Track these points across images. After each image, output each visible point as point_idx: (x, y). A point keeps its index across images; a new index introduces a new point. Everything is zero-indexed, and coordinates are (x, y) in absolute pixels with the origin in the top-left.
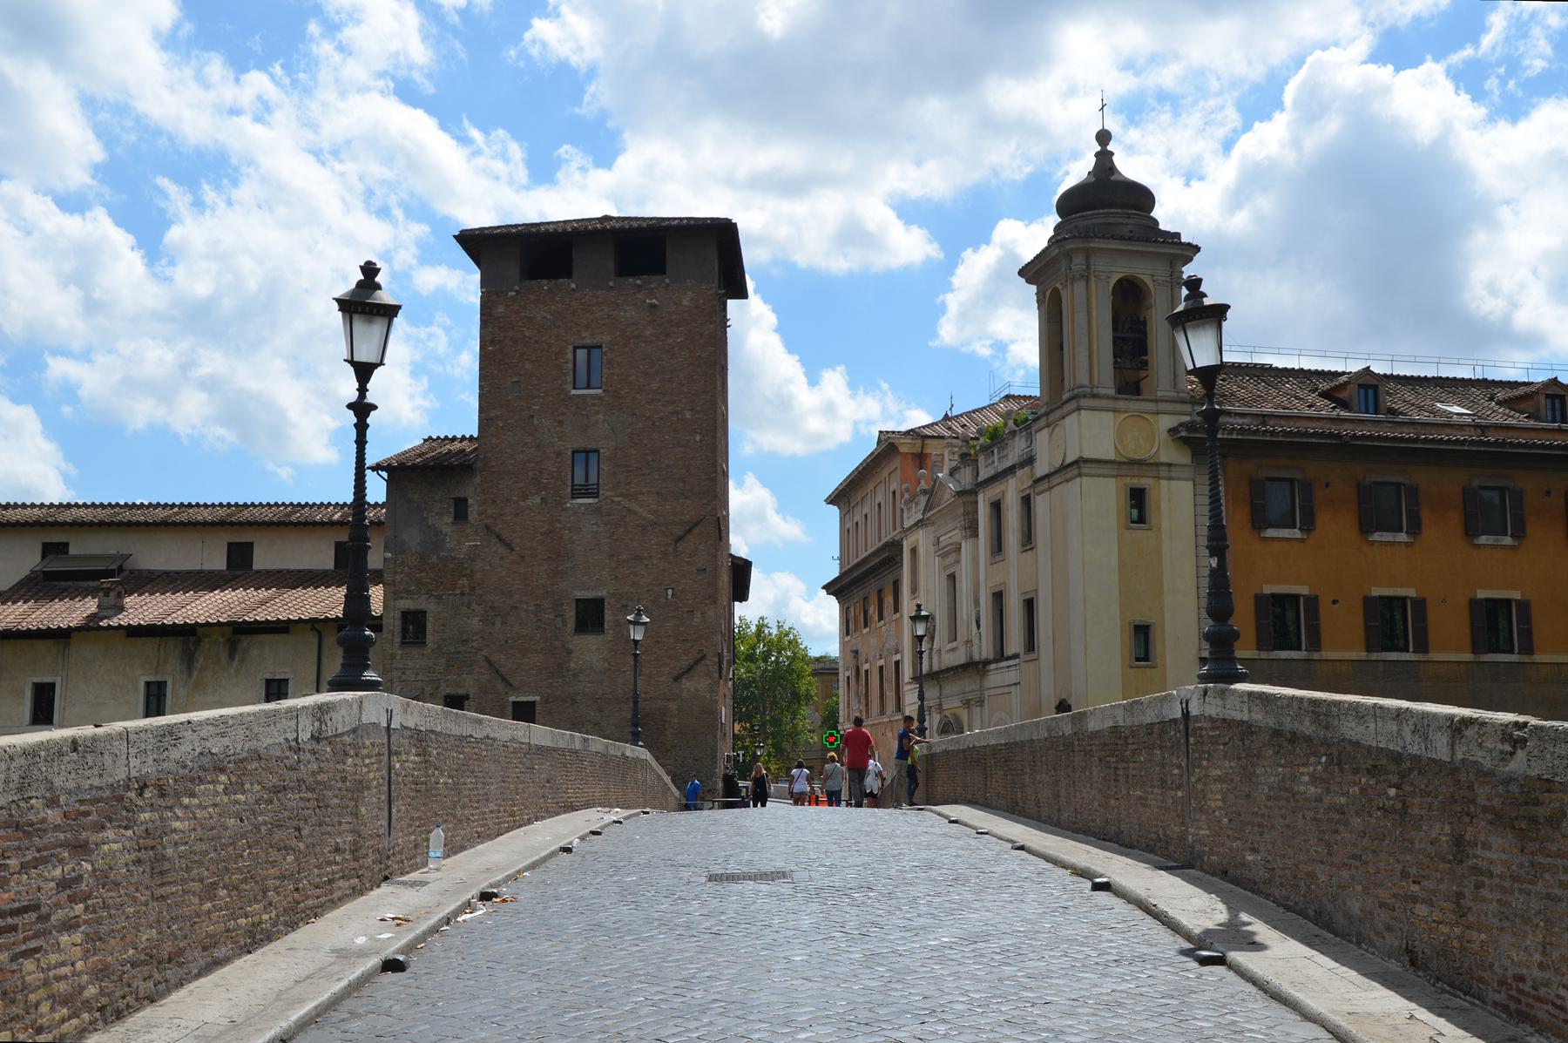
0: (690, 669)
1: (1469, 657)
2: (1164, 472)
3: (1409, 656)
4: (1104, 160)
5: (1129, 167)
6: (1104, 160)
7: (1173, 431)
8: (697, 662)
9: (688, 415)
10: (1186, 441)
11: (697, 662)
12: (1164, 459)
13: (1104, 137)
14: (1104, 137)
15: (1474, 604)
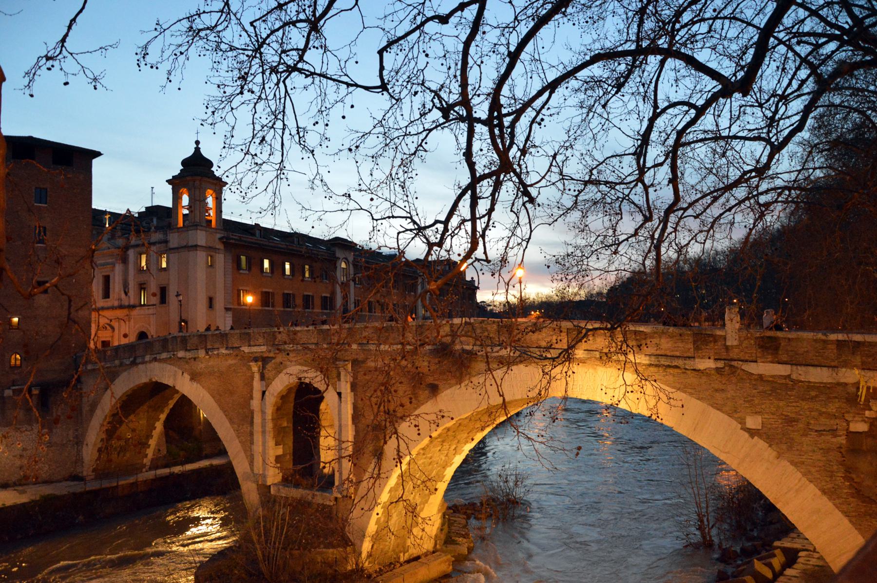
0: (82, 307)
1: (282, 309)
2: (217, 251)
3: (270, 308)
4: (197, 150)
5: (205, 153)
6: (197, 150)
7: (220, 239)
8: (85, 305)
9: (81, 218)
10: (223, 243)
11: (85, 305)
12: (217, 247)
13: (197, 143)
14: (197, 143)
15: (284, 294)
